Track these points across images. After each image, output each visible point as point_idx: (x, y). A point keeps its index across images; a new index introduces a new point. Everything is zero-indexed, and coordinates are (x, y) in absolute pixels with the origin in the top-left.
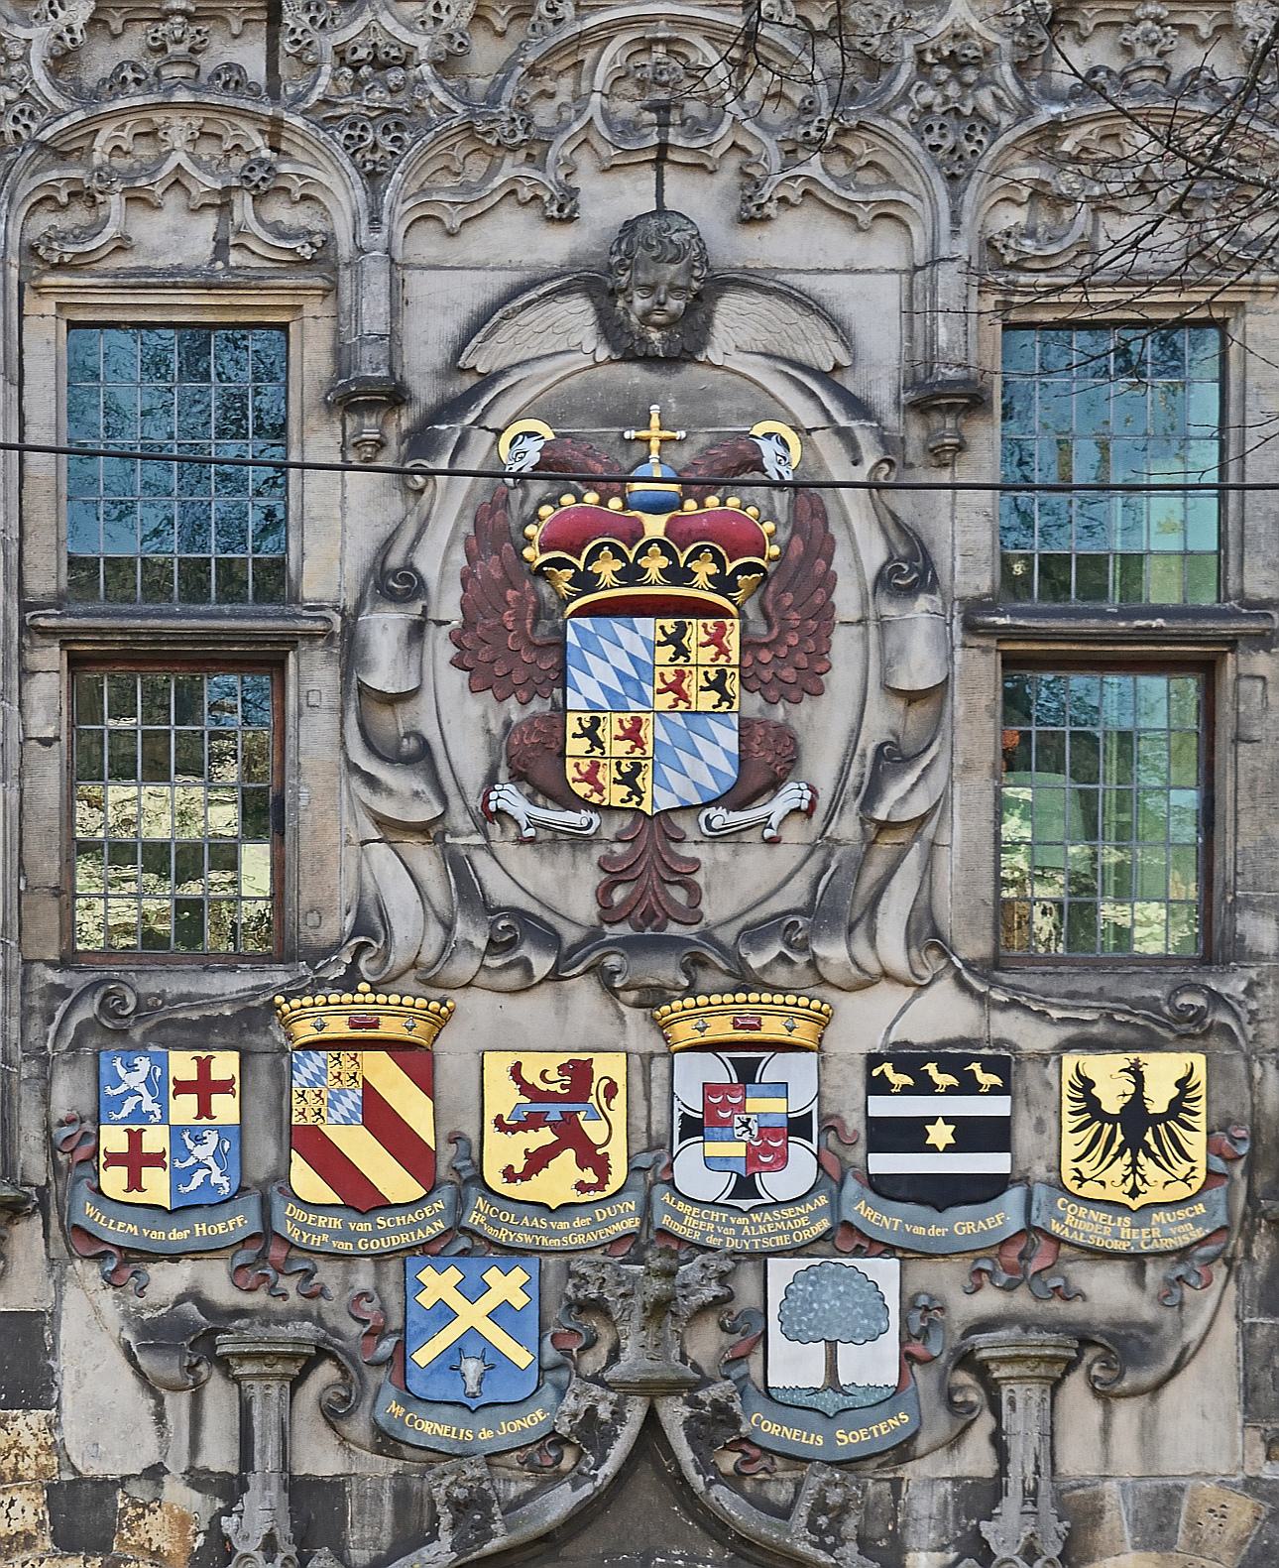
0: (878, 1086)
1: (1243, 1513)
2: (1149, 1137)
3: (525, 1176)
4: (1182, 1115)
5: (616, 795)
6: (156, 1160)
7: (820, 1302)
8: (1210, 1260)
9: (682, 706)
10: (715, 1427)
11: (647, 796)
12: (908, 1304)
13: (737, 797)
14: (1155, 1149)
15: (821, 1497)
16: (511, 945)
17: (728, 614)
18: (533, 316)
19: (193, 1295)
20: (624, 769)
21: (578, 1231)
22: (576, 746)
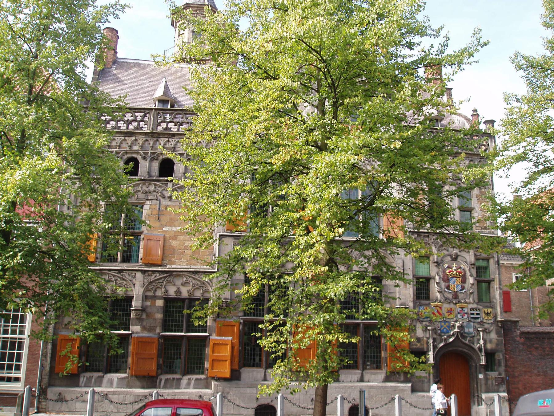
1: (496, 341)
13: (461, 290)
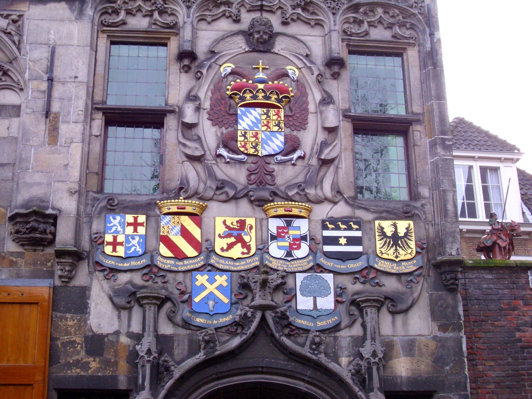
0: (325, 227)
1: (432, 345)
2: (400, 242)
3: (227, 250)
4: (408, 237)
5: (252, 151)
6: (121, 244)
7: (311, 286)
8: (419, 275)
9: (269, 130)
10: (283, 320)
11: (260, 152)
12: (336, 287)
14: (401, 245)
15: (313, 339)
16: (222, 188)
17: (280, 108)
18: (229, 39)
19: (130, 282)
20: (254, 145)
21: (242, 265)
22: (240, 139)
